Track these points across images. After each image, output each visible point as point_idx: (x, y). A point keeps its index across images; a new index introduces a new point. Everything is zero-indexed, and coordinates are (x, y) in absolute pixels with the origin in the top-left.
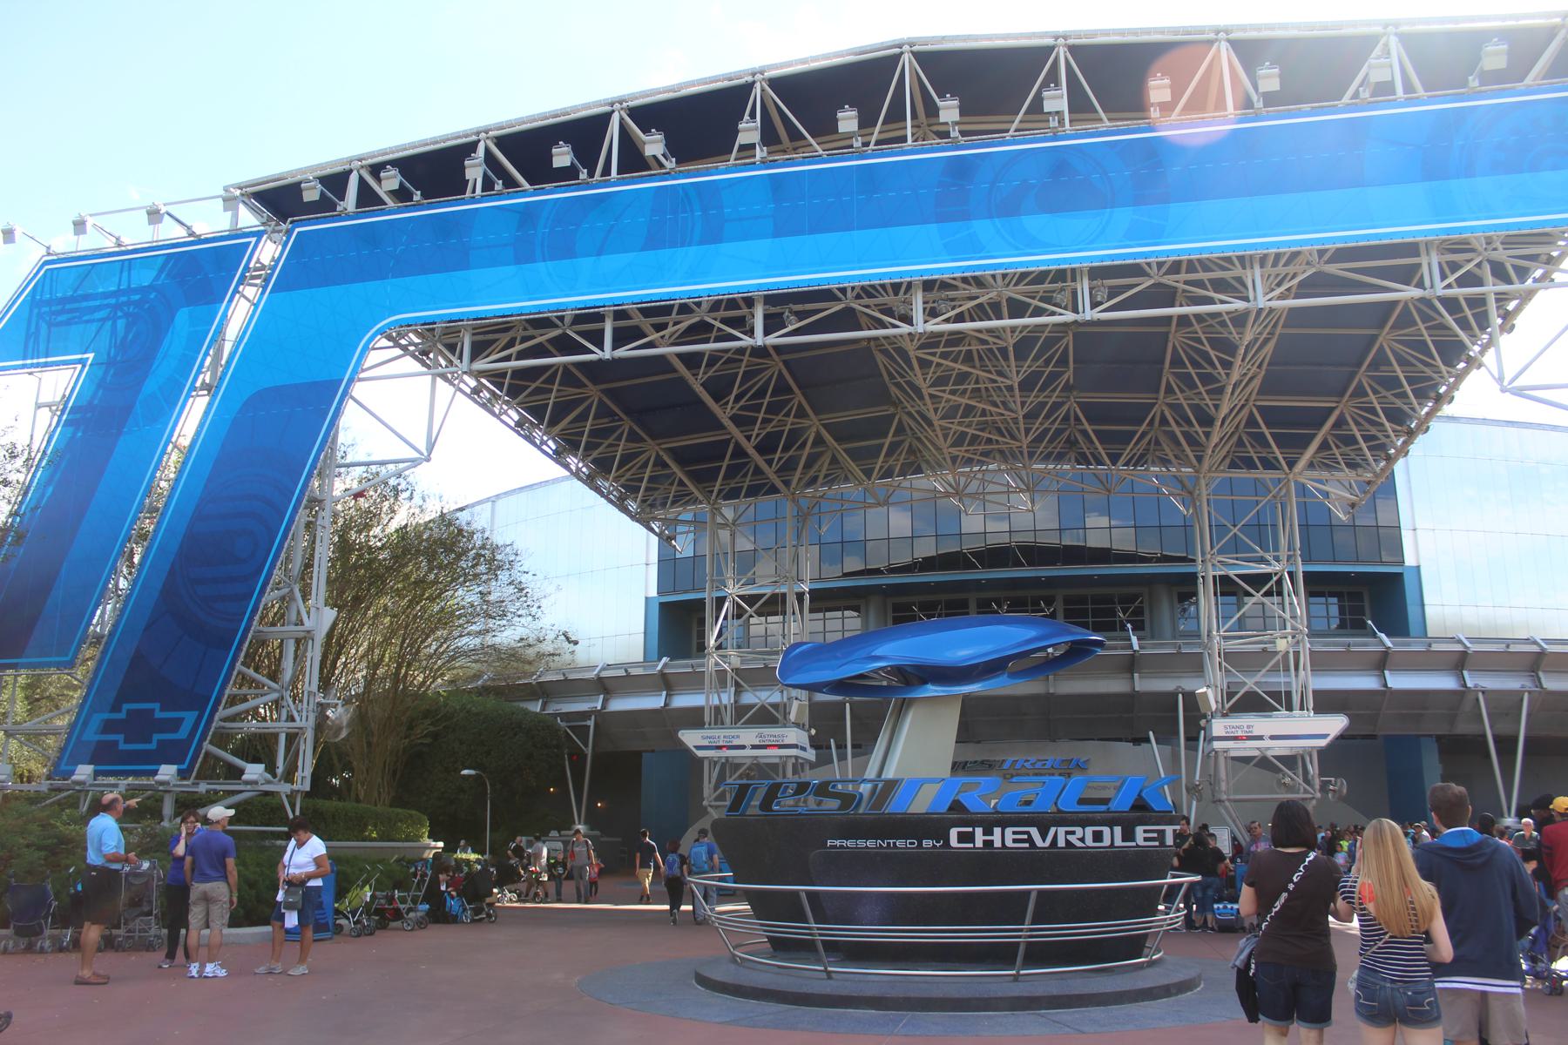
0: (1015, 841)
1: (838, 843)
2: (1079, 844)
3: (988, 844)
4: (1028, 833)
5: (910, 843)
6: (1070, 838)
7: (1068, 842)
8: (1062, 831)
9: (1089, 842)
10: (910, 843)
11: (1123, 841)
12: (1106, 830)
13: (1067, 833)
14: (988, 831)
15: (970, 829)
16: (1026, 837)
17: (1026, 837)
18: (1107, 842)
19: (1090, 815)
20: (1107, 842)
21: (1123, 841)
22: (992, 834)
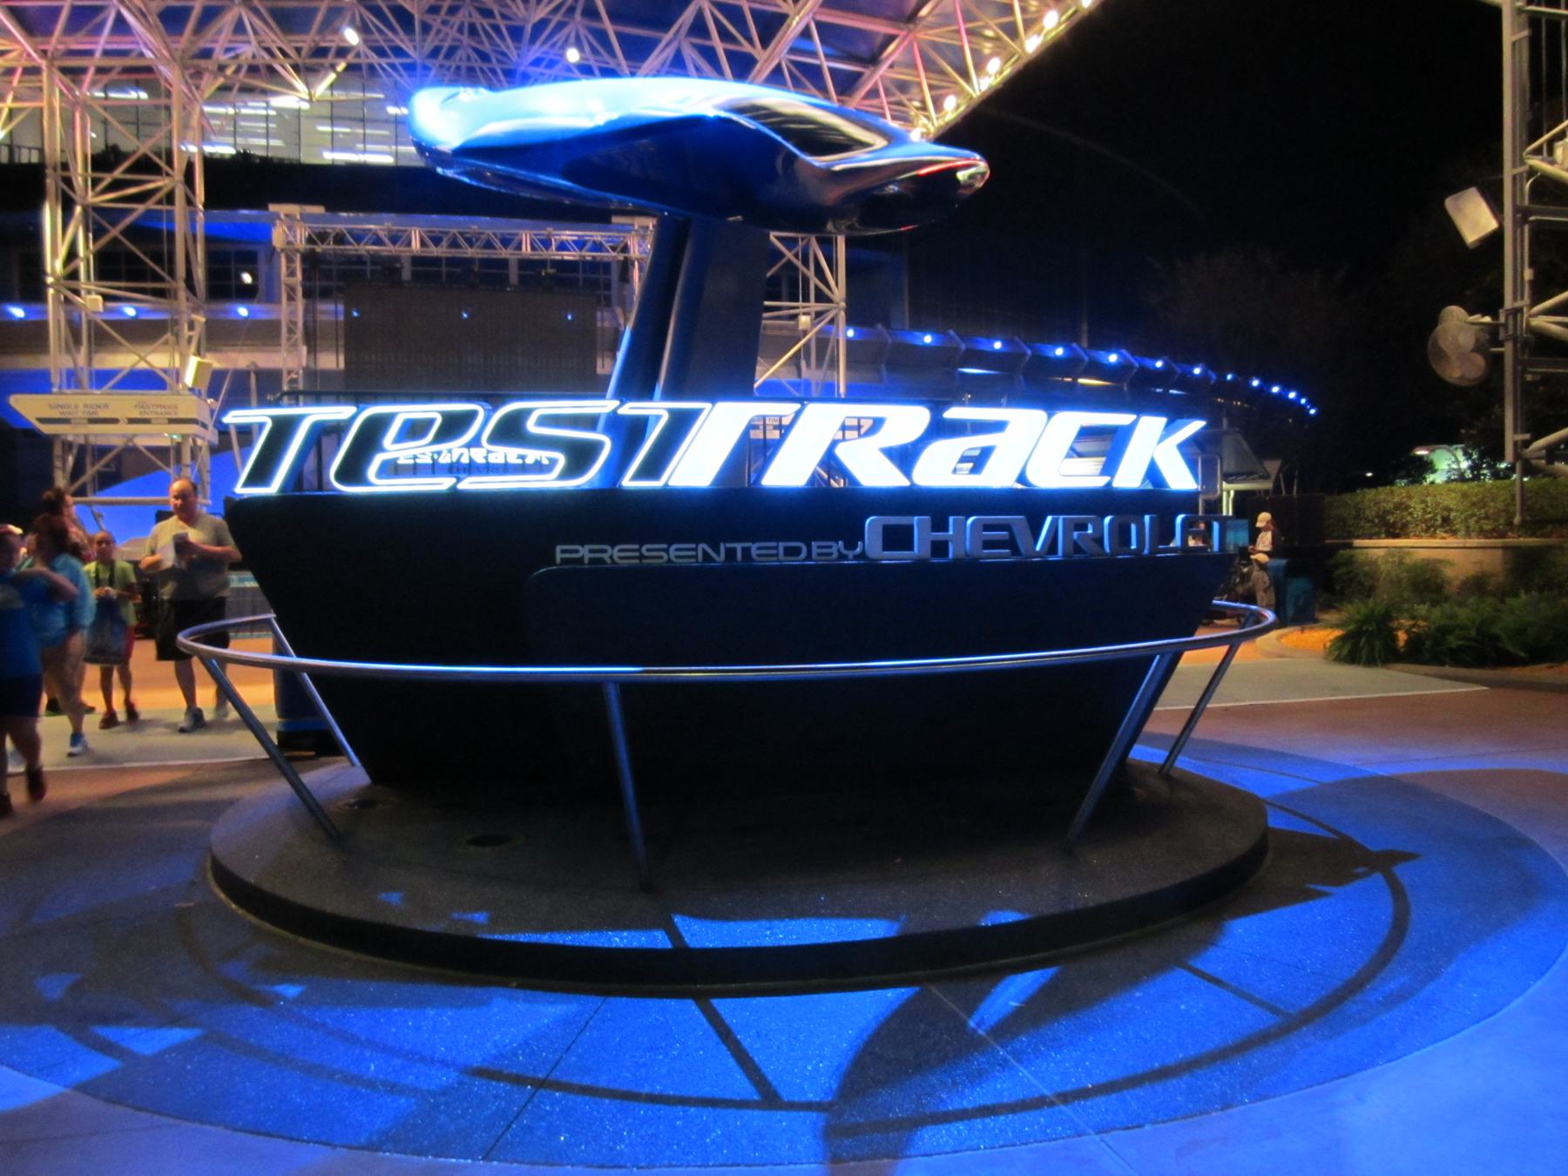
1: (584, 552)
3: (940, 548)
10: (797, 551)
16: (1004, 534)
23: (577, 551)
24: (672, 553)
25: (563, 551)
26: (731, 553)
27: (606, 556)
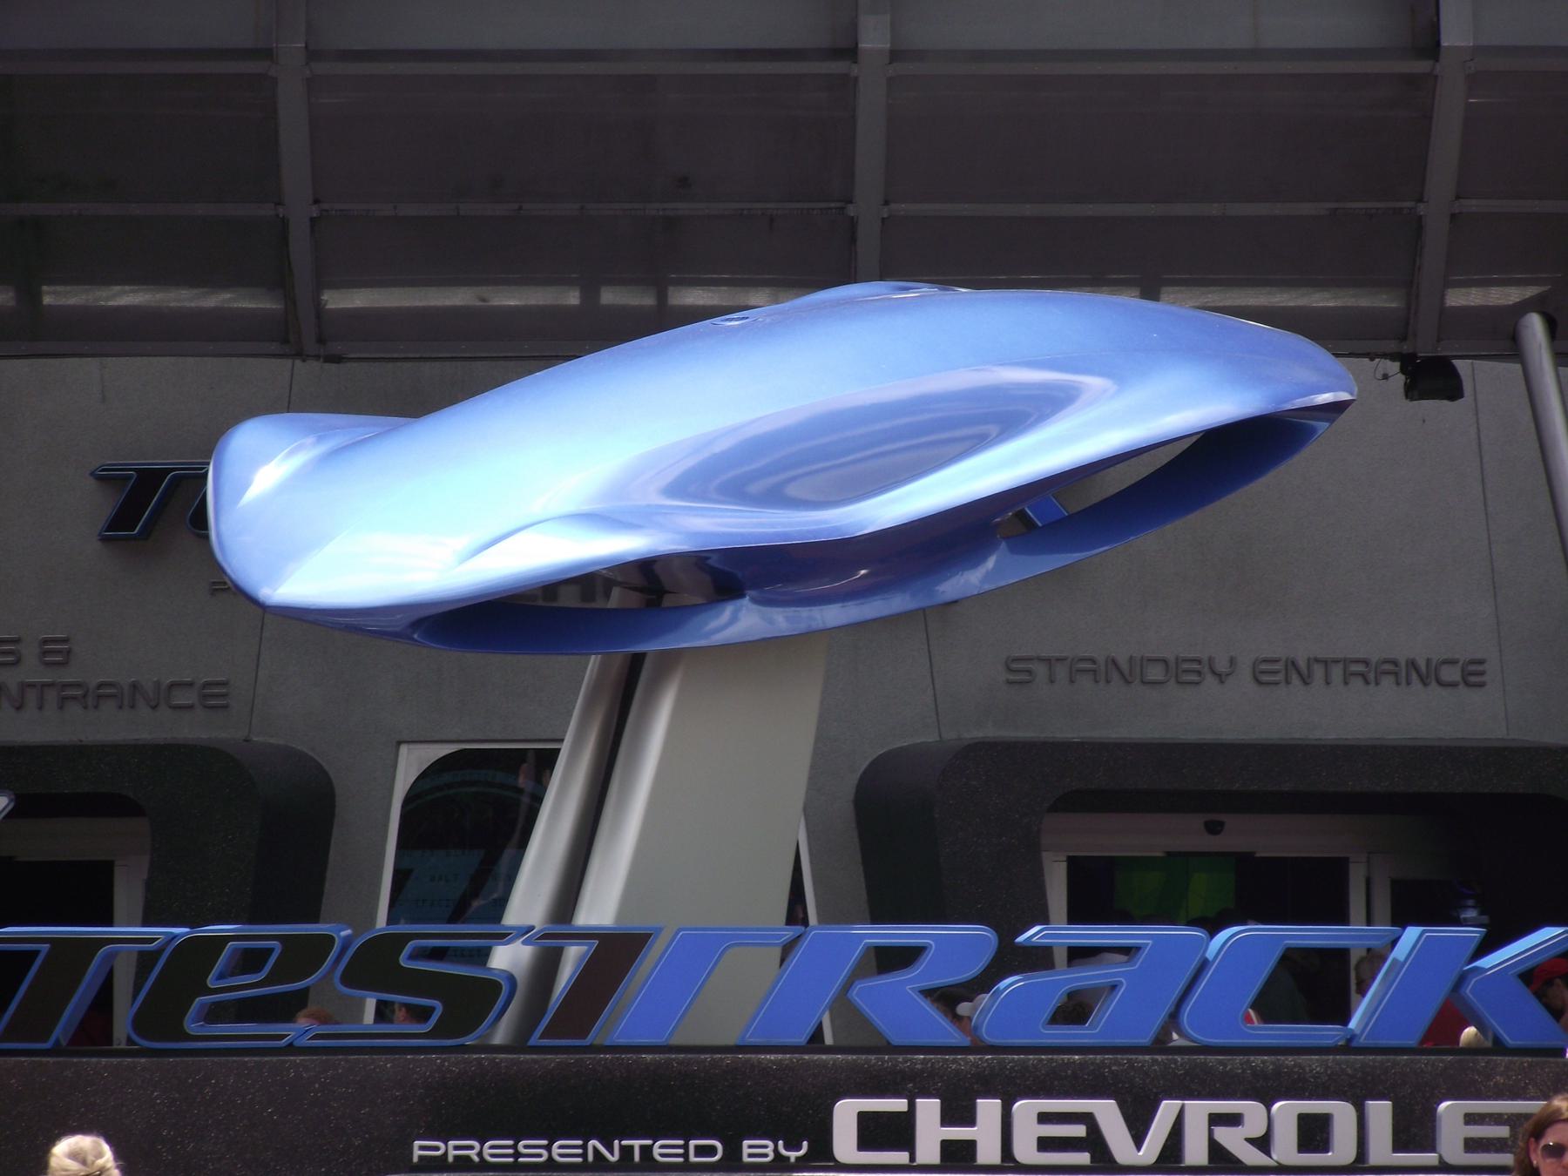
0: (1045, 1144)
2: (1252, 1156)
3: (958, 1154)
4: (1087, 1119)
5: (701, 1151)
6: (1224, 1135)
7: (1216, 1150)
8: (1198, 1110)
9: (1286, 1149)
10: (701, 1151)
11: (1399, 1146)
12: (1341, 1113)
13: (1216, 1120)
14: (958, 1112)
15: (899, 1105)
17: (1079, 1131)
18: (1342, 1150)
19: (1290, 1060)
20: (1342, 1150)
21: (1399, 1146)
22: (970, 1120)
23: (437, 1149)
24: (555, 1150)
25: (422, 1148)
26: (627, 1152)
27: (473, 1154)
